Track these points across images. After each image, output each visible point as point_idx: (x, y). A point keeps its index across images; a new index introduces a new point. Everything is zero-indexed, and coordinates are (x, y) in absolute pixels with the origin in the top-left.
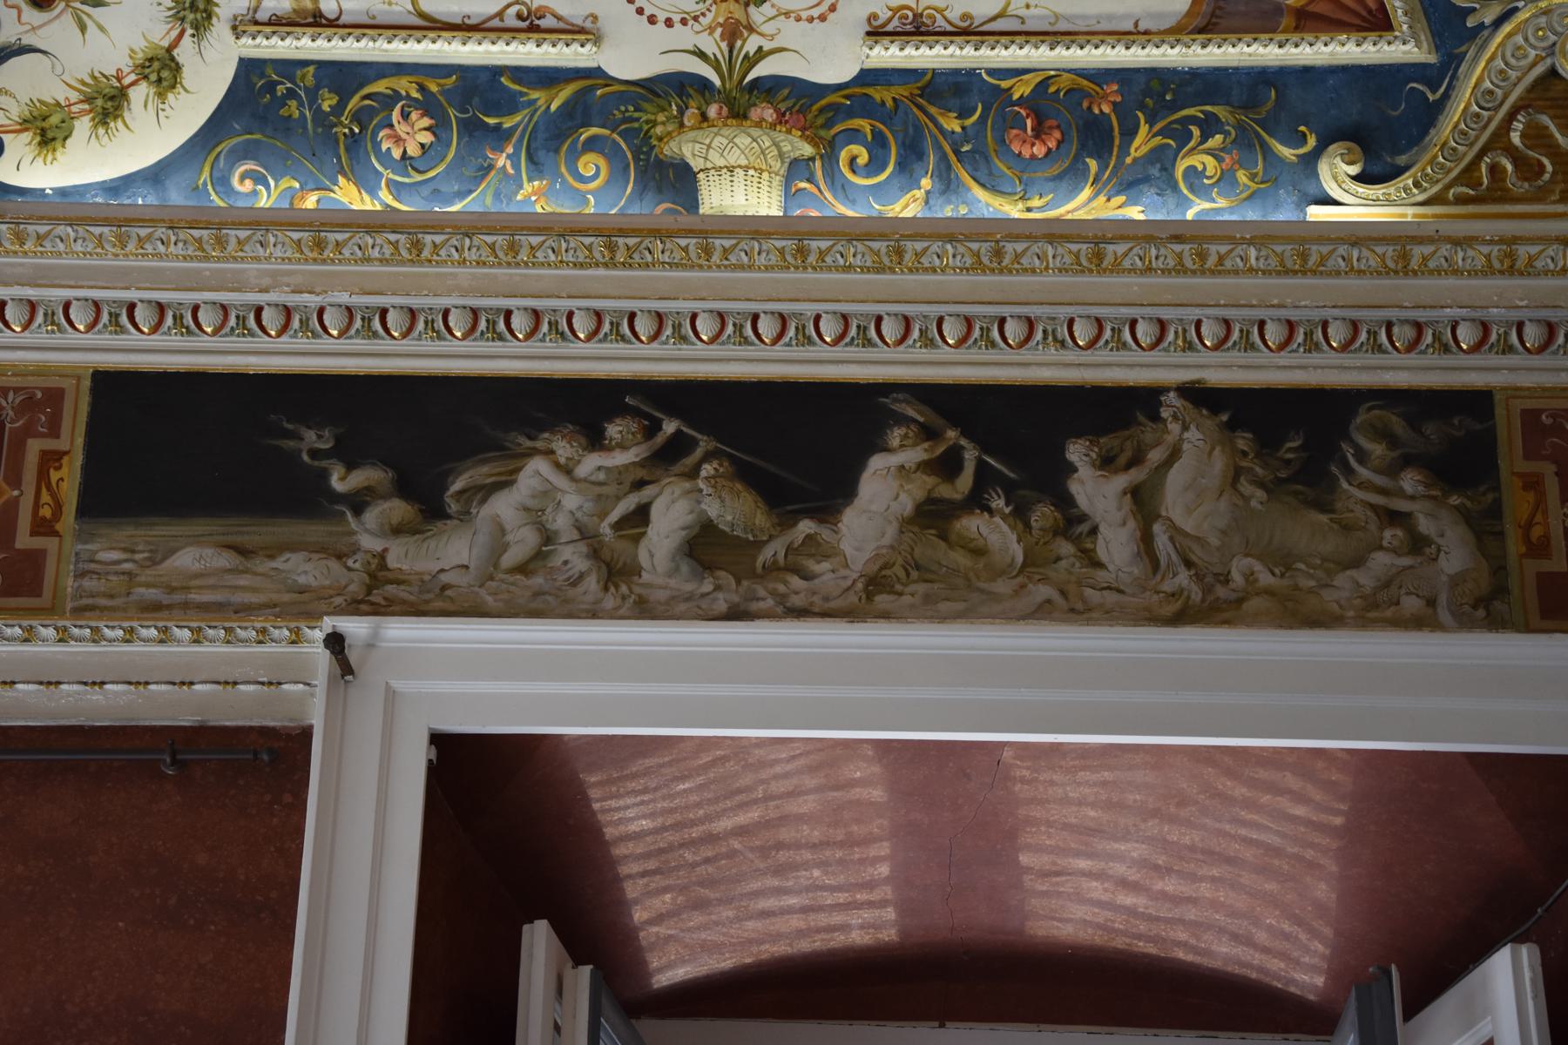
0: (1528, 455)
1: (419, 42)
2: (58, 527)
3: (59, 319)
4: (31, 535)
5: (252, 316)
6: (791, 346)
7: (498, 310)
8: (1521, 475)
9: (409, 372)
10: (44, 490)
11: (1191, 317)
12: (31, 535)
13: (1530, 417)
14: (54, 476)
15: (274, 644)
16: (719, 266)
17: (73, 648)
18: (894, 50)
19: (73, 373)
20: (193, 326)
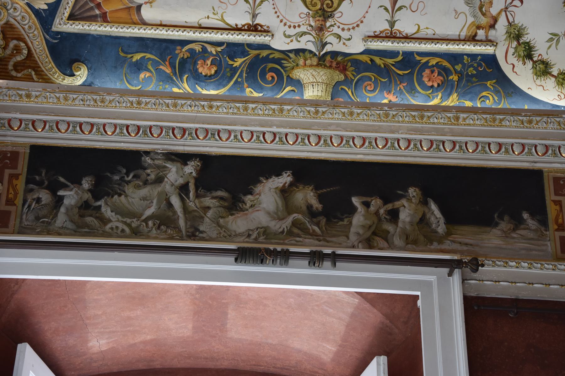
0: (556, 194)
1: (205, 33)
2: (15, 202)
3: (418, 146)
4: (6, 205)
5: (351, 140)
6: (322, 147)
7: (440, 141)
8: (553, 201)
9: (441, 164)
10: (11, 187)
11: (463, 141)
12: (6, 205)
13: (556, 180)
14: (15, 182)
15: (510, 267)
16: (498, 126)
17: (533, 271)
18: (417, 45)
19: (23, 145)
20: (263, 140)
